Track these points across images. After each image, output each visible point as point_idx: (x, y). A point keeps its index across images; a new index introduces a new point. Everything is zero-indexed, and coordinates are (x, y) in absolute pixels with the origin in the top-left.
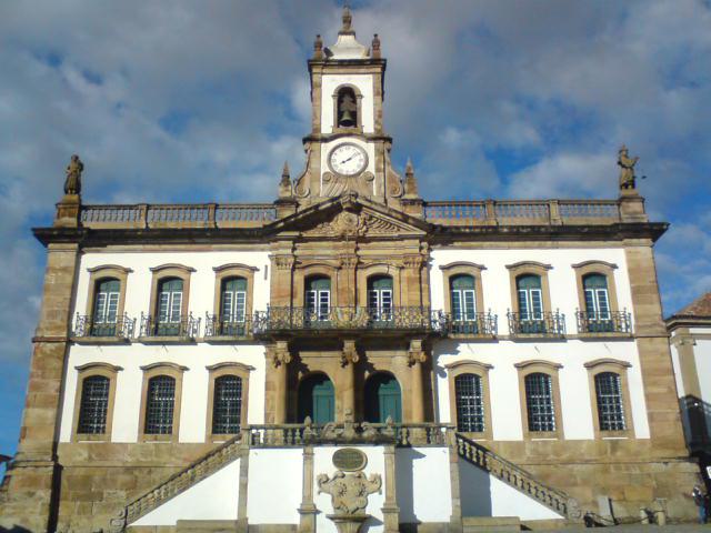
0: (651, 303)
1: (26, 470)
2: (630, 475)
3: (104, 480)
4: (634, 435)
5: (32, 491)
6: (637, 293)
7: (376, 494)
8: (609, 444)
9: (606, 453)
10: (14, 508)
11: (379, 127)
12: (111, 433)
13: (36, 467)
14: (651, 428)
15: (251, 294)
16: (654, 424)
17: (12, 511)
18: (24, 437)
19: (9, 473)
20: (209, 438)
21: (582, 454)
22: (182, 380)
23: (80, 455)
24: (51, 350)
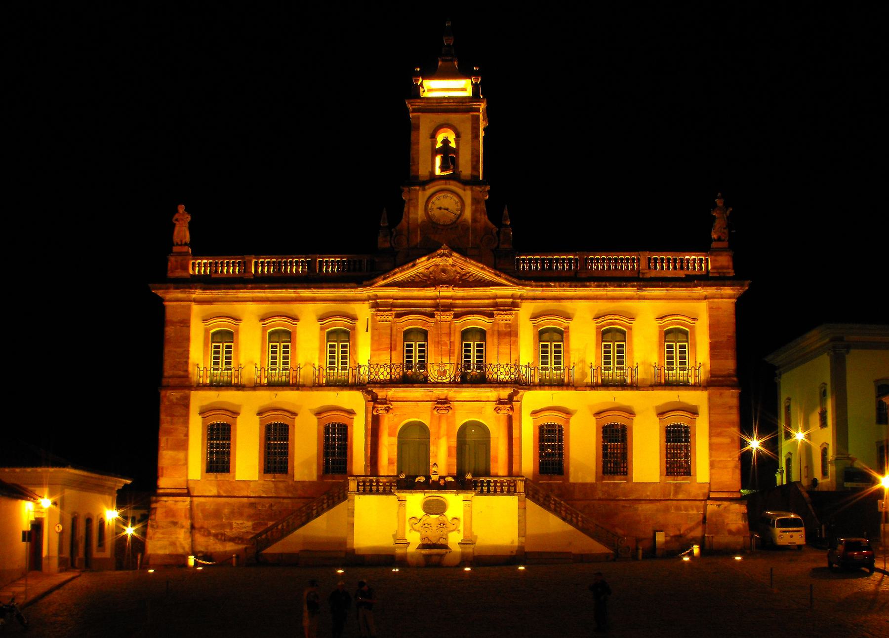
0: (726, 358)
1: (167, 503)
2: (689, 514)
3: (232, 513)
4: (696, 479)
5: (175, 521)
6: (714, 348)
7: (455, 533)
8: (672, 488)
9: (670, 495)
10: (163, 534)
11: (475, 174)
12: (235, 472)
13: (176, 501)
14: (711, 475)
15: (354, 346)
16: (713, 471)
17: (161, 536)
18: (162, 476)
19: (154, 506)
20: (320, 477)
21: (648, 496)
22: (294, 426)
23: (211, 491)
24: (177, 399)
